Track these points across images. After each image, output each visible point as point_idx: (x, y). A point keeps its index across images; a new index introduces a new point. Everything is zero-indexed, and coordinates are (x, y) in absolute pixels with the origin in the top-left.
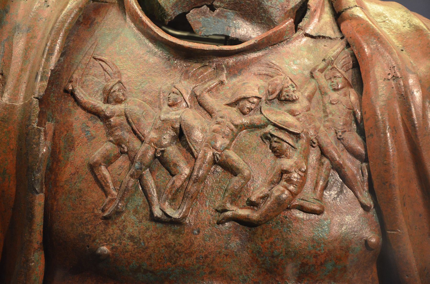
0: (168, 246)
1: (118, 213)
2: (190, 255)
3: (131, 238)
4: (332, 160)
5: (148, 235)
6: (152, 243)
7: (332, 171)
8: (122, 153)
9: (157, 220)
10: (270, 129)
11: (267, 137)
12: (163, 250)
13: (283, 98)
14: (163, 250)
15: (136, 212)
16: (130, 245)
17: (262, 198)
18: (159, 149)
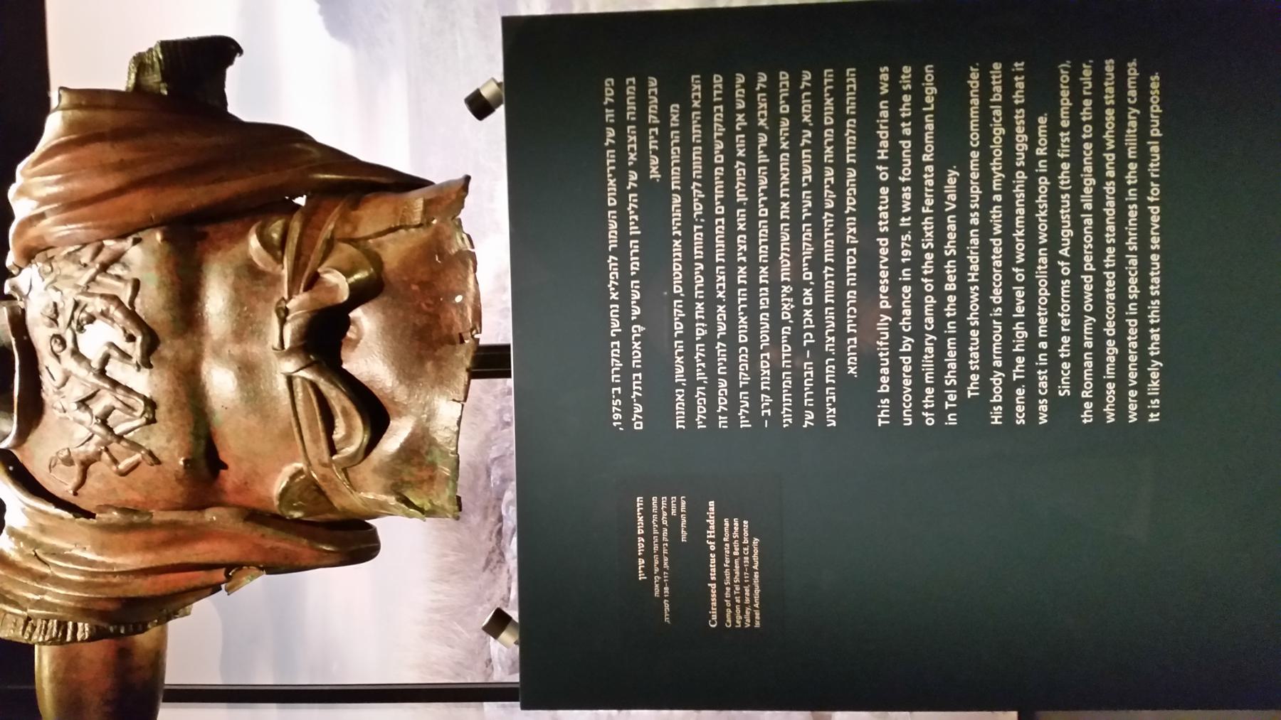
0: (170, 411)
1: (151, 453)
2: (176, 391)
3: (169, 441)
4: (98, 272)
5: (163, 428)
6: (170, 423)
7: (109, 271)
8: (107, 450)
9: (151, 421)
10: (74, 325)
11: (81, 329)
12: (175, 415)
13: (55, 315)
14: (175, 415)
15: (148, 438)
16: (175, 443)
17: (125, 331)
18: (95, 420)
